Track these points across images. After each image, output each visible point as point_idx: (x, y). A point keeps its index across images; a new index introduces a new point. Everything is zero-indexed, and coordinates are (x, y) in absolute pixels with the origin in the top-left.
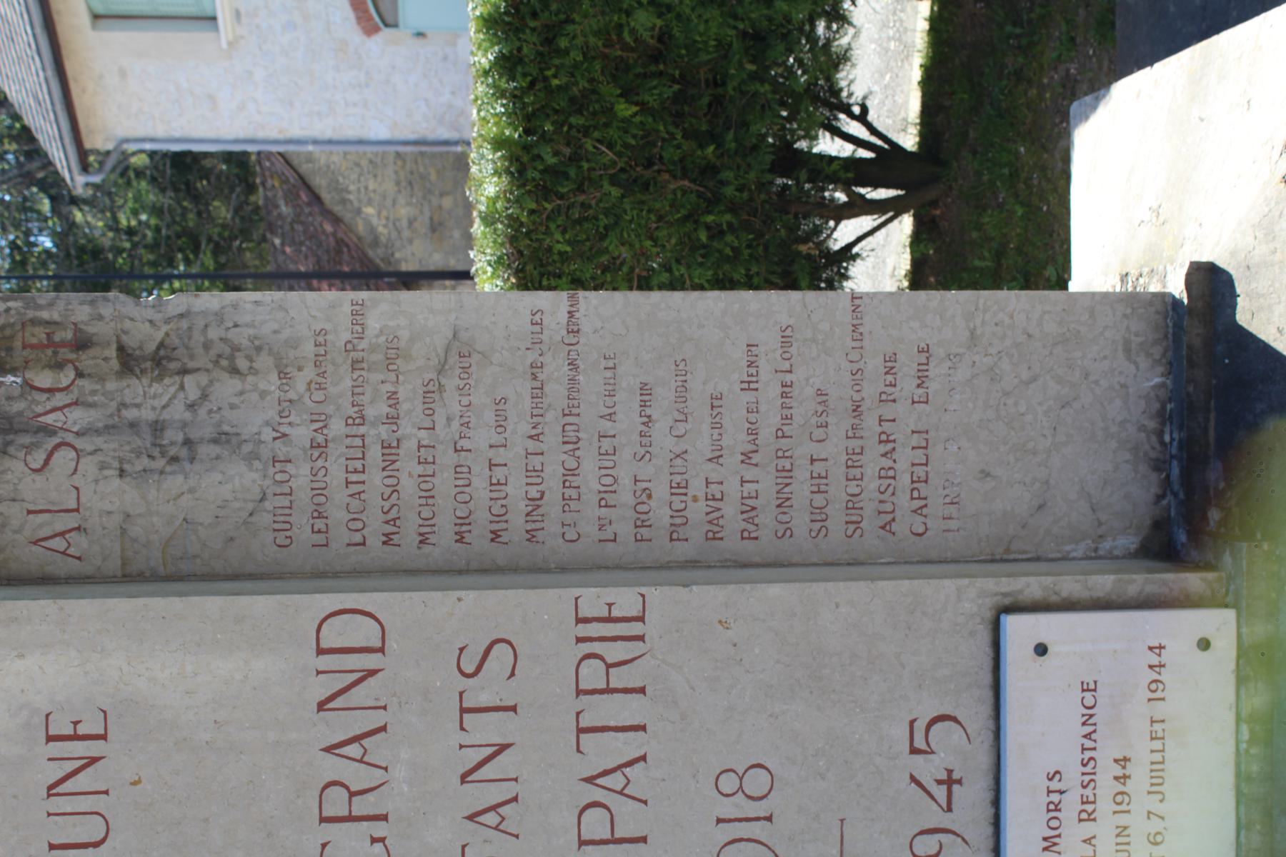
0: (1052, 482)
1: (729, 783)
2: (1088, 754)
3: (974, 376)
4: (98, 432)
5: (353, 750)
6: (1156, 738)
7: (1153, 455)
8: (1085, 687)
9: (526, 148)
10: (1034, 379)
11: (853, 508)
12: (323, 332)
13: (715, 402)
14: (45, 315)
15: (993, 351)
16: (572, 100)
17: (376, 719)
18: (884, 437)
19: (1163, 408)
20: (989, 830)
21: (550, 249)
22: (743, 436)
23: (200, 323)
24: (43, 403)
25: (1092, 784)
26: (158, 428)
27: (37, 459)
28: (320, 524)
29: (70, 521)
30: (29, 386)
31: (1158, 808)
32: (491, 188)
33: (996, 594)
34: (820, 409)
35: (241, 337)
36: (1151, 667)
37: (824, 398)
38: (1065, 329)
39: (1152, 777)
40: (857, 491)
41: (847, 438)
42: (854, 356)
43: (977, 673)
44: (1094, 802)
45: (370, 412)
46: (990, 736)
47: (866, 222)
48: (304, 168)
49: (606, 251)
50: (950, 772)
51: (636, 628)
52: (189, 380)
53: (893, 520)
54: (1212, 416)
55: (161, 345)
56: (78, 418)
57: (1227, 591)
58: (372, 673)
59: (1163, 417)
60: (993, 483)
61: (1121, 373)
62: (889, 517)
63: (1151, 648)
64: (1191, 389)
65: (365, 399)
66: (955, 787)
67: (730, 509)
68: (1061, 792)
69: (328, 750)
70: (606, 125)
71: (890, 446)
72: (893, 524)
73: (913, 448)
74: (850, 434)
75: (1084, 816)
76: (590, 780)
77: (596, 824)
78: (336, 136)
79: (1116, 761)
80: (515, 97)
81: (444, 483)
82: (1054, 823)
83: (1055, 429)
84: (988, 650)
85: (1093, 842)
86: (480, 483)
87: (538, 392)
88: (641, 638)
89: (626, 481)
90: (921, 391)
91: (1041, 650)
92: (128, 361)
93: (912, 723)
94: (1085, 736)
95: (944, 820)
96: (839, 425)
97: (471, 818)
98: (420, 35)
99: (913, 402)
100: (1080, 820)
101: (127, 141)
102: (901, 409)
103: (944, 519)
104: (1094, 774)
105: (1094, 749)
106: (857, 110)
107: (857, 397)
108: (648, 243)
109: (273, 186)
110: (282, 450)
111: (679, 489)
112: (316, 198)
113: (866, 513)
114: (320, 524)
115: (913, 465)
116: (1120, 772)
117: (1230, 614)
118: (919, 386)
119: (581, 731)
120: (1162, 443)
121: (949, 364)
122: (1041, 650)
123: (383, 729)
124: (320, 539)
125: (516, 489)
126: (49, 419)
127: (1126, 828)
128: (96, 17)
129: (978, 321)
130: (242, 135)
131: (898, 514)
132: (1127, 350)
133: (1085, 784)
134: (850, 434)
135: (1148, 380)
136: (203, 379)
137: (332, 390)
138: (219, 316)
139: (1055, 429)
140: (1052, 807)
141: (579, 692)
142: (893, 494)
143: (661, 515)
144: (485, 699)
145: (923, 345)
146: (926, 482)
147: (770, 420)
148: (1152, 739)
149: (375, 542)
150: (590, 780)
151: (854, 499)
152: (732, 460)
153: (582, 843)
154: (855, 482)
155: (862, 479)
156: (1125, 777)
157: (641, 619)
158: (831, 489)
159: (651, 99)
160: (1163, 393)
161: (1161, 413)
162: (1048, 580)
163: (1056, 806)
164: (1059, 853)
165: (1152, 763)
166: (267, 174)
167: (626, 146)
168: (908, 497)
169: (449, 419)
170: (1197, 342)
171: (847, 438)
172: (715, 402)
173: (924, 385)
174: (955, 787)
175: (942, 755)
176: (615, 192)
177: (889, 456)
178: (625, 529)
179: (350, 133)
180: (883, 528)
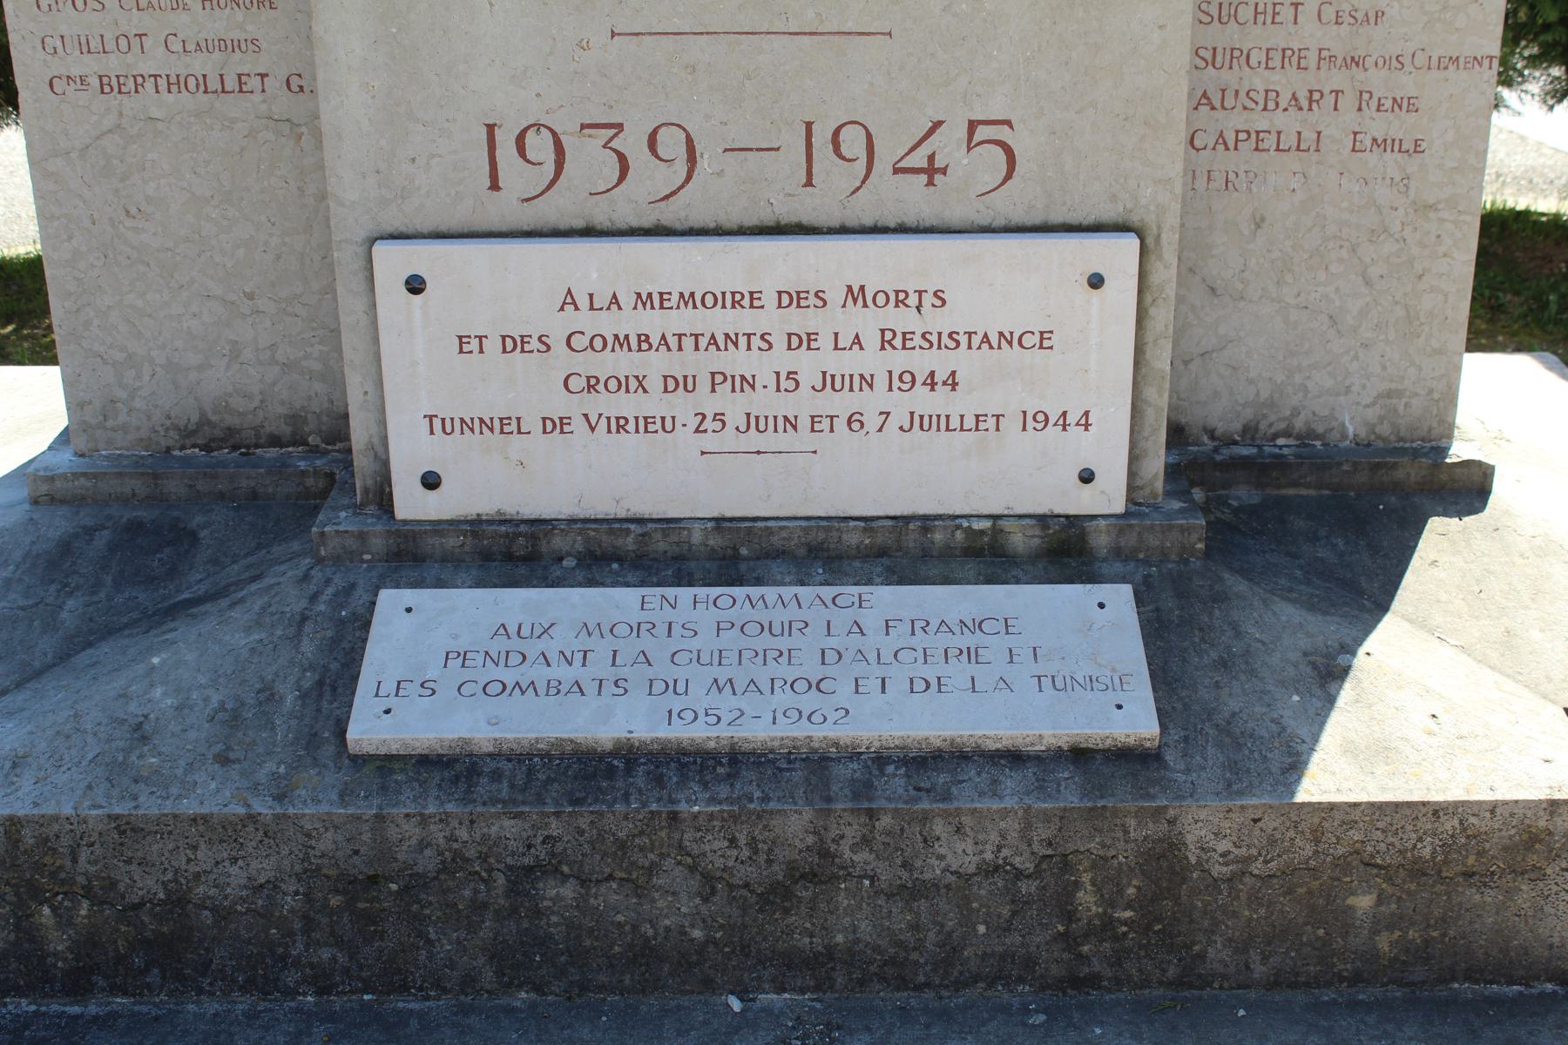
0: (1242, 304)
2: (964, 340)
3: (1379, 210)
6: (977, 421)
7: (1263, 426)
8: (1046, 335)
10: (1368, 283)
11: (1232, 57)
15: (1407, 232)
18: (1316, 96)
19: (1317, 437)
20: (868, 221)
25: (926, 345)
31: (893, 423)
33: (1159, 227)
34: (1360, 15)
36: (1064, 414)
37: (1372, 20)
38: (1423, 320)
39: (931, 417)
40: (1253, 62)
41: (1320, 50)
42: (1421, 59)
43: (1065, 204)
44: (904, 348)
46: (985, 222)
50: (944, 171)
53: (1213, 108)
54: (1312, 492)
57: (1140, 504)
59: (1308, 435)
60: (1246, 232)
61: (1364, 387)
62: (1217, 104)
63: (1086, 414)
64: (1346, 467)
66: (924, 178)
68: (918, 308)
71: (1305, 104)
72: (1208, 108)
73: (1299, 133)
74: (1324, 54)
75: (888, 335)
79: (953, 373)
82: (881, 299)
83: (1306, 308)
84: (1090, 219)
85: (856, 347)
90: (1368, 143)
91: (1096, 282)
93: (1008, 123)
94: (986, 335)
95: (883, 164)
96: (1336, 39)
99: (1355, 134)
100: (883, 331)
102: (1348, 117)
103: (1209, 172)
104: (939, 347)
105: (970, 347)
107: (1369, 62)
113: (1225, 75)
115: (1279, 133)
116: (939, 378)
117: (1119, 507)
118: (1375, 140)
120: (1276, 436)
121: (1397, 179)
122: (1096, 282)
127: (871, 386)
129: (1445, 215)
131: (1220, 114)
132: (1389, 394)
133: (928, 336)
134: (1324, 54)
135: (1352, 418)
139: (1306, 308)
140: (901, 296)
142: (1245, 108)
145: (1424, 145)
146: (1257, 149)
148: (977, 416)
151: (1244, 58)
154: (1264, 59)
155: (1267, 68)
156: (933, 385)
158: (1258, 29)
160: (1334, 437)
161: (1311, 434)
162: (1171, 291)
163: (902, 302)
164: (844, 306)
165: (948, 417)
168: (1240, 127)
170: (1400, 474)
171: (1320, 50)
173: (1375, 147)
174: (924, 178)
175: (965, 162)
177: (1293, 103)
180: (1205, 95)
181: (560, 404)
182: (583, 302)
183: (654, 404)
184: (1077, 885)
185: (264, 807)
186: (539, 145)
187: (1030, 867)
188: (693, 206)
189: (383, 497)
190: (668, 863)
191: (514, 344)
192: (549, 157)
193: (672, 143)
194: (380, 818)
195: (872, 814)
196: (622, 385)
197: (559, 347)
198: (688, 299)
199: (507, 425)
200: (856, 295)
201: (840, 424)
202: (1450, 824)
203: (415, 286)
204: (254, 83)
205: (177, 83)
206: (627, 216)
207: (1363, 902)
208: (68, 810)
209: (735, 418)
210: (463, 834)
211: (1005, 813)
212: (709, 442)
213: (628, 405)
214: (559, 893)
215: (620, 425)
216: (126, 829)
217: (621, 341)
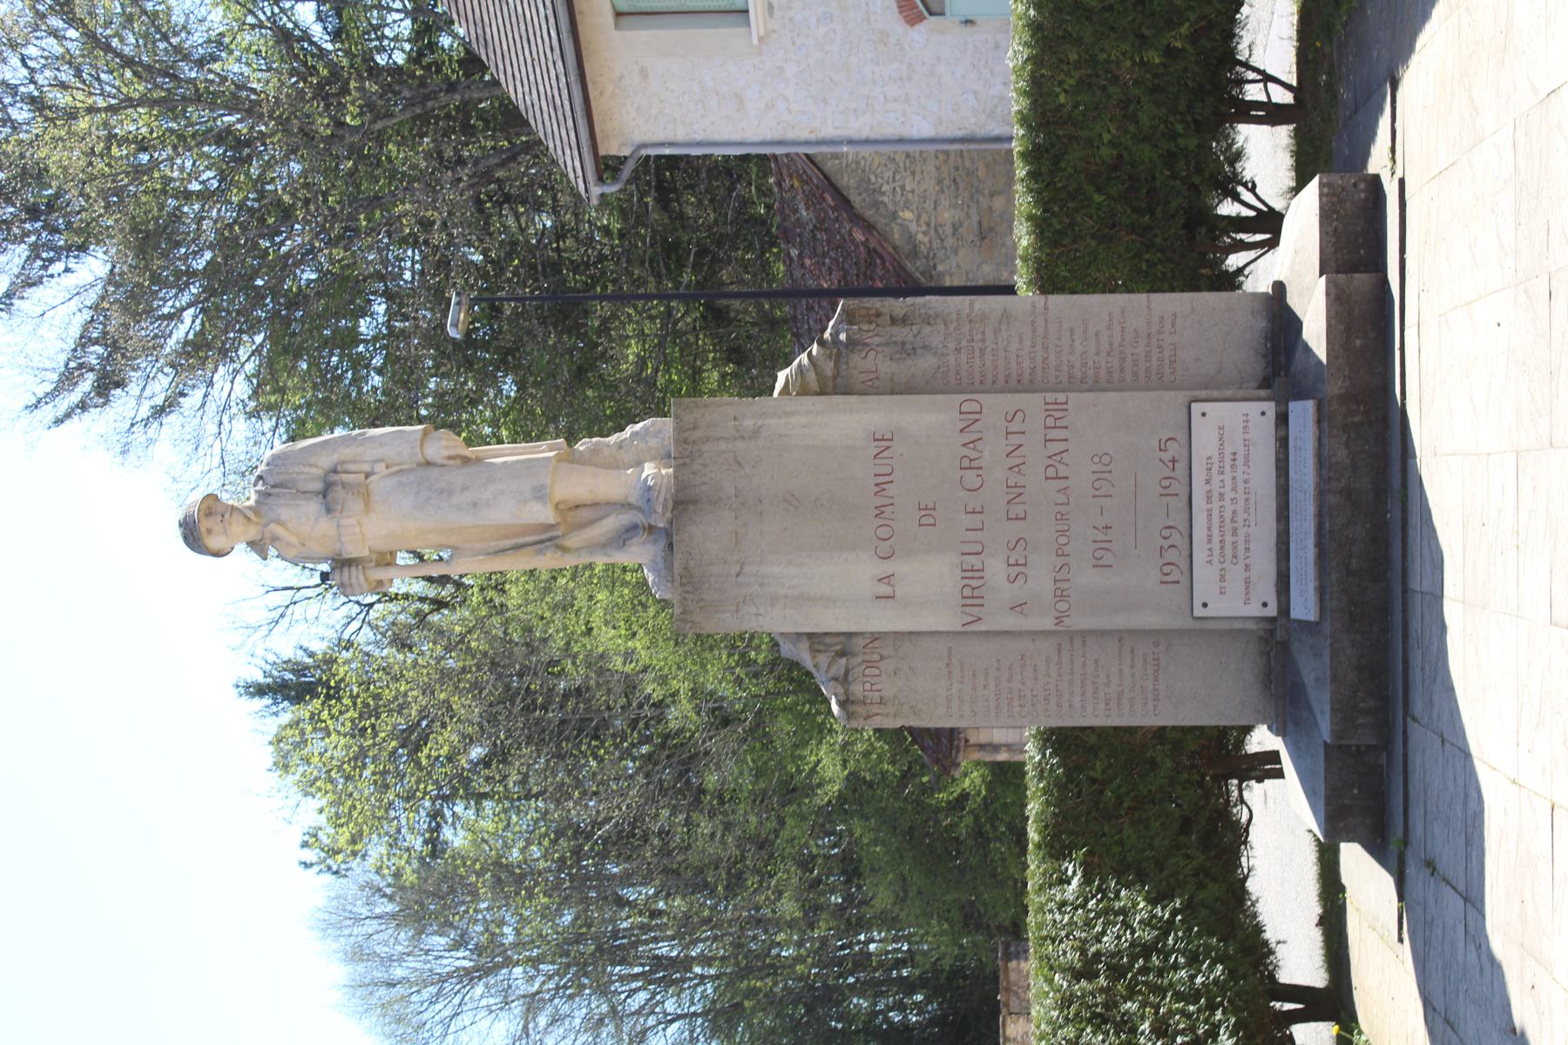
5: (971, 446)
9: (1044, 220)
13: (1097, 334)
16: (1069, 194)
17: (978, 436)
21: (1058, 275)
26: (903, 343)
27: (863, 354)
29: (874, 376)
32: (1024, 242)
35: (932, 312)
45: (976, 338)
47: (1252, 254)
48: (829, 166)
49: (1089, 275)
51: (1064, 407)
52: (914, 327)
56: (877, 340)
59: (1266, 337)
67: (1103, 372)
70: (1089, 206)
78: (873, 135)
80: (1039, 192)
81: (1001, 363)
87: (1034, 331)
91: (1204, 414)
92: (894, 321)
95: (1172, 474)
98: (969, 22)
101: (645, 146)
106: (1250, 185)
109: (792, 186)
110: (945, 351)
111: (1085, 364)
112: (844, 202)
117: (1273, 404)
125: (1026, 365)
128: (619, 14)
130: (769, 137)
138: (924, 305)
143: (1078, 374)
144: (1014, 429)
147: (1117, 340)
149: (977, 383)
153: (1047, 478)
159: (1113, 192)
161: (1266, 337)
166: (785, 172)
167: (1099, 217)
172: (1097, 334)
176: (1093, 243)
178: (1064, 379)
179: (890, 131)
181: (1241, 566)
183: (1241, 539)
185: (1328, 642)
186: (1167, 569)
188: (1184, 528)
191: (1222, 578)
192: (1170, 567)
193: (1166, 533)
195: (1329, 478)
196: (1235, 548)
198: (1209, 529)
199: (1247, 582)
203: (1205, 605)
206: (1187, 546)
207: (1358, 343)
209: (1245, 516)
212: (1252, 523)
213: (1241, 547)
214: (1354, 563)
215: (1247, 549)
216: (1334, 679)
217: (1222, 548)
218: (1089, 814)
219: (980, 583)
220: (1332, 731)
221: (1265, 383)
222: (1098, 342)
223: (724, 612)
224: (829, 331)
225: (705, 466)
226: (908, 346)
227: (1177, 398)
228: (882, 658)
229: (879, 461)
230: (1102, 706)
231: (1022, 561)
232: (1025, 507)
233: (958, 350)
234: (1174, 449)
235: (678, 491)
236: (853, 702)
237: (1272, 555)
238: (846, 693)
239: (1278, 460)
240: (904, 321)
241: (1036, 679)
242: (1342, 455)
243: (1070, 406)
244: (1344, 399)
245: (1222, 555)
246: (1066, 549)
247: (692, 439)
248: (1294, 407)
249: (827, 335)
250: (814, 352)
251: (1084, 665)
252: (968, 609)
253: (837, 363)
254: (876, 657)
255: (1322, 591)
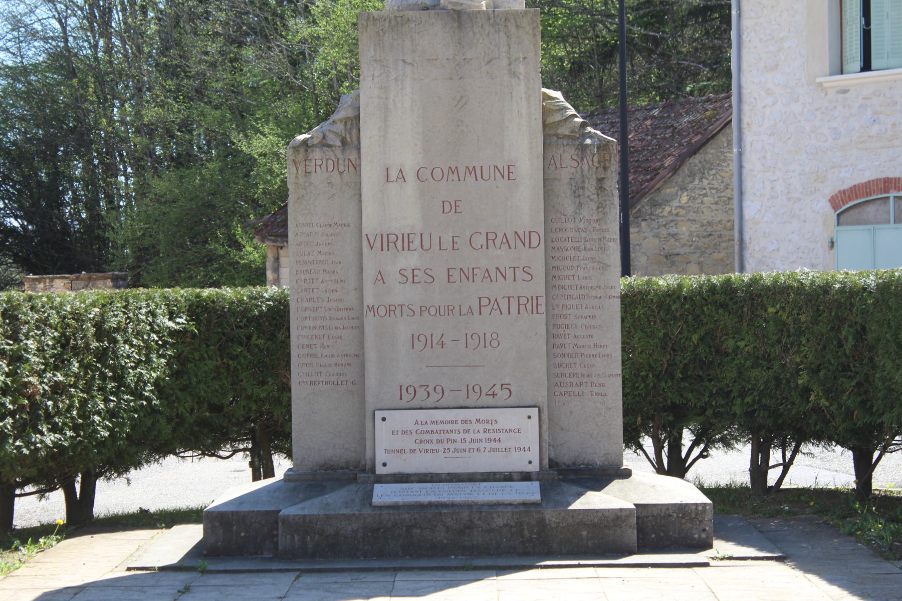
1: (495, 336)
4: (582, 173)
5: (505, 240)
9: (679, 297)
10: (598, 427)
12: (609, 231)
13: (591, 336)
14: (612, 159)
16: (698, 316)
17: (512, 246)
21: (636, 308)
22: (581, 344)
23: (611, 199)
24: (589, 158)
26: (583, 188)
27: (575, 157)
28: (558, 230)
29: (558, 166)
30: (594, 155)
32: (661, 282)
35: (607, 209)
42: (604, 375)
45: (587, 243)
48: (722, 138)
51: (535, 312)
52: (596, 196)
55: (605, 189)
56: (586, 168)
58: (524, 245)
59: (588, 464)
65: (591, 242)
67: (561, 341)
69: (505, 234)
70: (689, 331)
76: (496, 300)
77: (485, 302)
78: (745, 172)
81: (568, 263)
86: (568, 272)
88: (532, 313)
89: (569, 312)
91: (529, 417)
92: (600, 180)
95: (483, 393)
97: (487, 270)
98: (832, 245)
106: (705, 454)
108: (640, 350)
109: (707, 110)
111: (567, 327)
112: (694, 150)
114: (558, 230)
117: (538, 470)
119: (509, 298)
123: (510, 248)
124: (554, 230)
125: (567, 282)
126: (585, 160)
130: (745, 91)
132: (606, 454)
136: (596, 200)
137: (593, 233)
138: (612, 204)
141: (519, 297)
143: (560, 321)
144: (517, 273)
149: (553, 245)
150: (496, 300)
152: (575, 341)
153: (480, 298)
157: (537, 313)
159: (700, 350)
166: (718, 104)
167: (681, 339)
169: (585, 264)
172: (591, 336)
176: (661, 335)
178: (556, 312)
179: (748, 185)
181: (414, 446)
182: (420, 423)
183: (434, 446)
184: (524, 529)
186: (411, 390)
187: (514, 525)
188: (443, 402)
189: (373, 470)
190: (439, 524)
191: (404, 432)
193: (439, 389)
194: (380, 514)
195: (481, 512)
197: (414, 433)
198: (442, 422)
199: (402, 451)
200: (478, 421)
201: (475, 450)
202: (600, 514)
203: (384, 419)
204: (345, 383)
205: (327, 383)
206: (429, 405)
207: (584, 533)
208: (316, 513)
209: (452, 449)
210: (397, 518)
211: (508, 512)
212: (446, 455)
213: (429, 446)
216: (328, 517)
217: (428, 432)
218: (224, 334)
219: (399, 247)
220: (289, 516)
221: (553, 464)
222: (584, 337)
223: (375, 50)
224: (593, 131)
225: (488, 35)
226: (581, 192)
227: (542, 397)
228: (341, 173)
229: (493, 170)
230: (306, 342)
231: (416, 279)
232: (458, 282)
233: (578, 230)
234: (503, 394)
235: (469, 14)
236: (306, 151)
237: (422, 470)
238: (313, 146)
239: (495, 473)
240: (601, 188)
241: (326, 291)
242: (499, 522)
243: (535, 315)
244: (542, 523)
245: (423, 432)
246: (426, 314)
247: (509, 24)
248: (535, 486)
249: (589, 129)
250: (576, 120)
251: (336, 328)
252: (379, 238)
253: (569, 137)
254: (341, 169)
255: (395, 507)
